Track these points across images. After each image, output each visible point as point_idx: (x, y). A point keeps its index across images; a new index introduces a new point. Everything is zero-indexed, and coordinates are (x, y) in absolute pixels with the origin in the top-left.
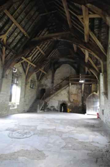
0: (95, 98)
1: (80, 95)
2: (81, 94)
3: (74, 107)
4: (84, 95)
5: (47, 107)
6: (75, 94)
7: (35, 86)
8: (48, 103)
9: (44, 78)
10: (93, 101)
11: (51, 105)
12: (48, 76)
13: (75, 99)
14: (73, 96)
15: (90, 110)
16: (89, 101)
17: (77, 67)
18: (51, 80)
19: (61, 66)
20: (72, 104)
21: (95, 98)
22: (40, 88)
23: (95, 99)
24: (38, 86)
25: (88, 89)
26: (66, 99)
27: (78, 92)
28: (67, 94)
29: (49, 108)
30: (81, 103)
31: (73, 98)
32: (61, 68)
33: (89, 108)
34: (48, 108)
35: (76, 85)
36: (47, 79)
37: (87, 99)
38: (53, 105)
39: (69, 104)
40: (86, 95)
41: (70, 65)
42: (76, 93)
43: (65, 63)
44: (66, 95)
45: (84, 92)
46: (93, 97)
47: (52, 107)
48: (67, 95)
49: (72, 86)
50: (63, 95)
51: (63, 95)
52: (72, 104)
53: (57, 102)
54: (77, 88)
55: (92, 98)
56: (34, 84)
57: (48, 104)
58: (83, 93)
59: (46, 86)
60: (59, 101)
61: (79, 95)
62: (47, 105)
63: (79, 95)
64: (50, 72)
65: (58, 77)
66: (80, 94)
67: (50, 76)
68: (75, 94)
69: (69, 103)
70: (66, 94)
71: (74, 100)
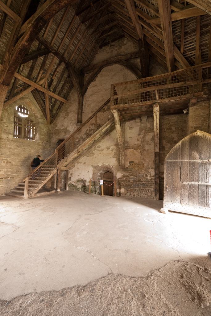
0: (200, 153)
1: (153, 148)
2: (152, 145)
3: (132, 181)
4: (162, 147)
5: (69, 183)
6: (136, 147)
7: (40, 134)
8: (71, 171)
9: (62, 114)
10: (194, 164)
11: (77, 178)
12: (70, 106)
13: (136, 161)
14: (129, 151)
15: (179, 197)
16: (174, 165)
17: (140, 68)
18: (77, 115)
19: (99, 75)
20: (126, 174)
21: (200, 153)
22: (55, 139)
23: (200, 158)
24: (50, 135)
25: (174, 129)
26: (112, 162)
27: (144, 140)
28: (113, 147)
29: (73, 183)
30: (153, 173)
31: (133, 155)
32: (98, 79)
33: (174, 190)
34: (71, 185)
35: (138, 120)
36: (67, 115)
37: (166, 159)
38: (82, 177)
39: (119, 175)
40: (167, 146)
41: (123, 65)
42: (139, 142)
43: (108, 63)
44: (112, 151)
45: (161, 138)
46: (191, 149)
47: (79, 181)
48: (114, 151)
49: (128, 124)
50: (105, 151)
51: (105, 151)
52: (126, 174)
53: (91, 169)
54: (141, 130)
55: (187, 152)
56: (38, 129)
57: (71, 174)
58: (157, 140)
59: (66, 131)
60: (95, 167)
61: (147, 147)
62: (69, 176)
63: (147, 147)
64: (74, 96)
65: (92, 105)
66: (150, 145)
67: (74, 107)
68: (136, 147)
69: (118, 170)
70: (111, 147)
71: (130, 162)
